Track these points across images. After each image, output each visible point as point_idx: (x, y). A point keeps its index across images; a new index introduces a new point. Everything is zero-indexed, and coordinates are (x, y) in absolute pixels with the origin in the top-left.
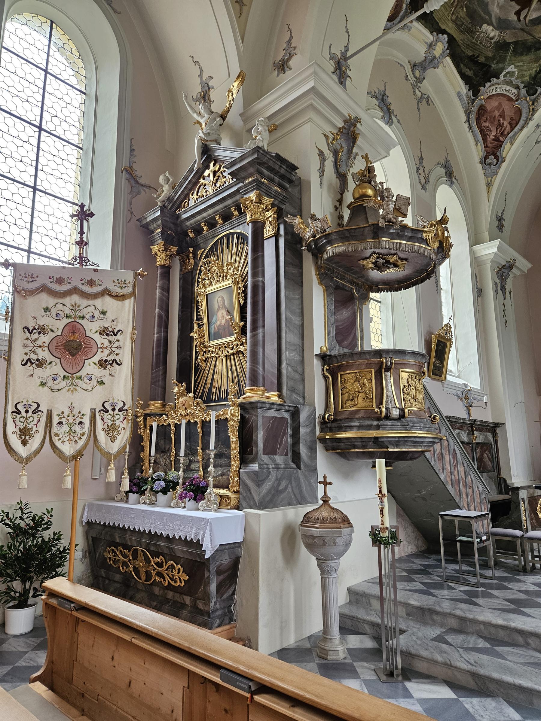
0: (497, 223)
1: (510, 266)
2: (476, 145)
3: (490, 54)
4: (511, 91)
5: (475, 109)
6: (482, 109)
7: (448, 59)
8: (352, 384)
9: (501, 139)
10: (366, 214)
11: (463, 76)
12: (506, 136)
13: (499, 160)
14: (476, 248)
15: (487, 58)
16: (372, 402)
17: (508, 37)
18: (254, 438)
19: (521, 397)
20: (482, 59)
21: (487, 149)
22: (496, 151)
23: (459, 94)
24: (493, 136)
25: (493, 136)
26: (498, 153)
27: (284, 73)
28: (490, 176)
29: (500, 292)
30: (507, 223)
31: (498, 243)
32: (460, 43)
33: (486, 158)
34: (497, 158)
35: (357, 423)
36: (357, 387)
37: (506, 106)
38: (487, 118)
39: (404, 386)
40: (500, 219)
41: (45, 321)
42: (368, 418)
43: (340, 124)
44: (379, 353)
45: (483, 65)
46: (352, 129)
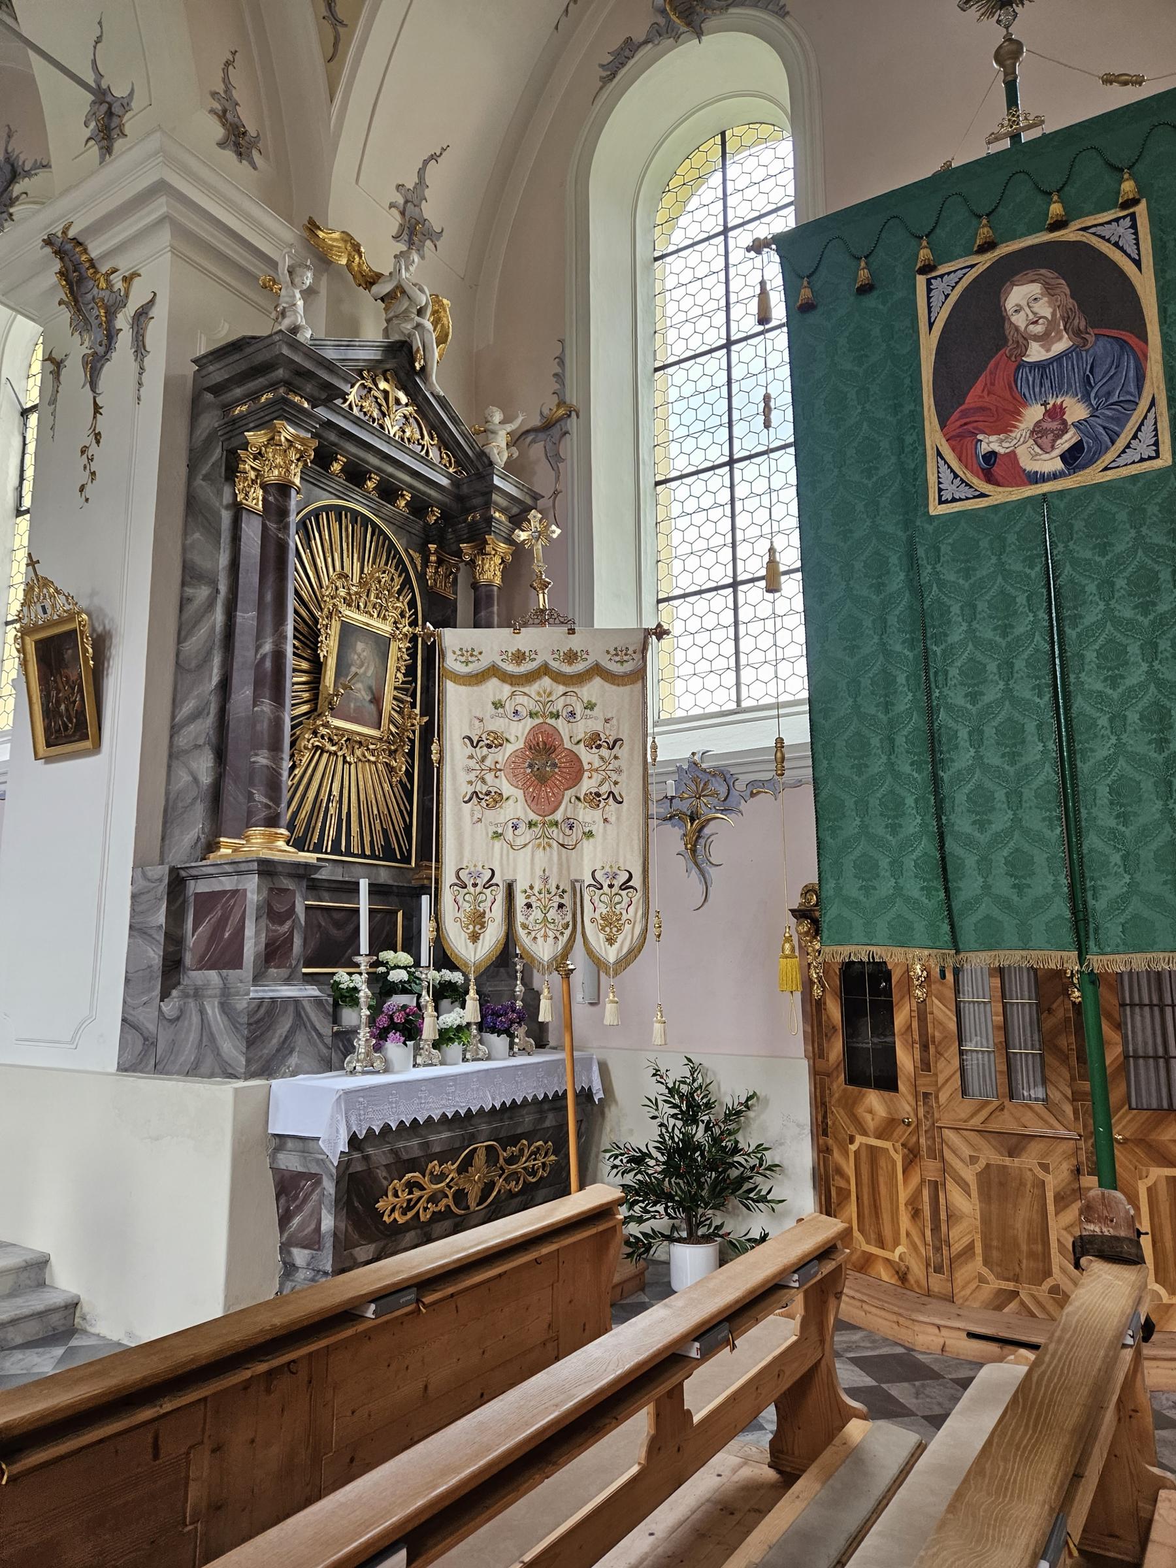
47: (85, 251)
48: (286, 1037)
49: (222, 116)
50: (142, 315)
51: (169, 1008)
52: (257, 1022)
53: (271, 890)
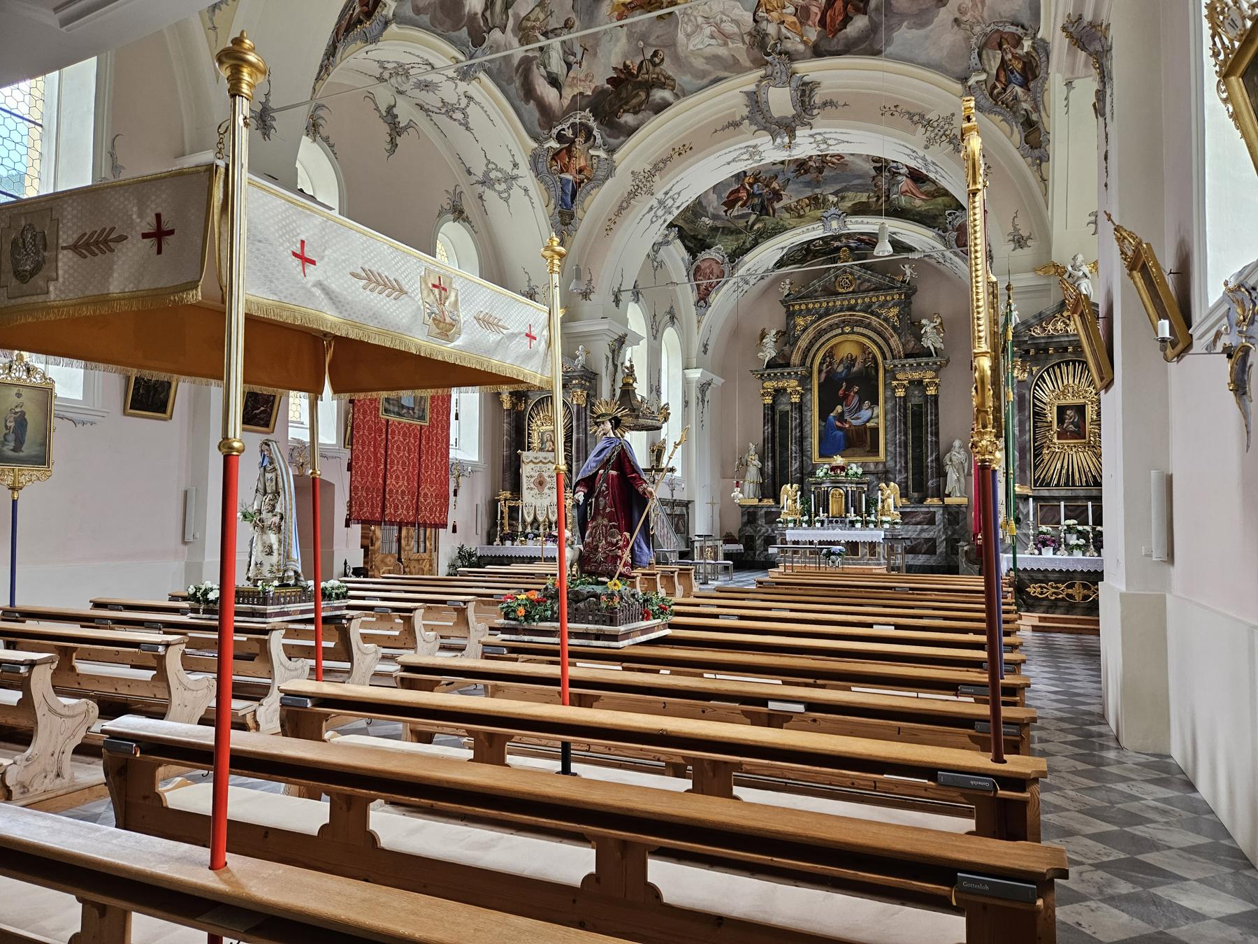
3: (706, 234)
4: (719, 258)
5: (694, 267)
6: (698, 268)
7: (678, 241)
11: (687, 248)
13: (707, 305)
15: (704, 236)
17: (719, 224)
19: (708, 482)
20: (700, 237)
23: (683, 259)
28: (701, 315)
29: (700, 403)
32: (686, 229)
33: (698, 302)
34: (706, 303)
37: (715, 266)
40: (705, 346)
41: (533, 473)
43: (616, 337)
45: (701, 240)
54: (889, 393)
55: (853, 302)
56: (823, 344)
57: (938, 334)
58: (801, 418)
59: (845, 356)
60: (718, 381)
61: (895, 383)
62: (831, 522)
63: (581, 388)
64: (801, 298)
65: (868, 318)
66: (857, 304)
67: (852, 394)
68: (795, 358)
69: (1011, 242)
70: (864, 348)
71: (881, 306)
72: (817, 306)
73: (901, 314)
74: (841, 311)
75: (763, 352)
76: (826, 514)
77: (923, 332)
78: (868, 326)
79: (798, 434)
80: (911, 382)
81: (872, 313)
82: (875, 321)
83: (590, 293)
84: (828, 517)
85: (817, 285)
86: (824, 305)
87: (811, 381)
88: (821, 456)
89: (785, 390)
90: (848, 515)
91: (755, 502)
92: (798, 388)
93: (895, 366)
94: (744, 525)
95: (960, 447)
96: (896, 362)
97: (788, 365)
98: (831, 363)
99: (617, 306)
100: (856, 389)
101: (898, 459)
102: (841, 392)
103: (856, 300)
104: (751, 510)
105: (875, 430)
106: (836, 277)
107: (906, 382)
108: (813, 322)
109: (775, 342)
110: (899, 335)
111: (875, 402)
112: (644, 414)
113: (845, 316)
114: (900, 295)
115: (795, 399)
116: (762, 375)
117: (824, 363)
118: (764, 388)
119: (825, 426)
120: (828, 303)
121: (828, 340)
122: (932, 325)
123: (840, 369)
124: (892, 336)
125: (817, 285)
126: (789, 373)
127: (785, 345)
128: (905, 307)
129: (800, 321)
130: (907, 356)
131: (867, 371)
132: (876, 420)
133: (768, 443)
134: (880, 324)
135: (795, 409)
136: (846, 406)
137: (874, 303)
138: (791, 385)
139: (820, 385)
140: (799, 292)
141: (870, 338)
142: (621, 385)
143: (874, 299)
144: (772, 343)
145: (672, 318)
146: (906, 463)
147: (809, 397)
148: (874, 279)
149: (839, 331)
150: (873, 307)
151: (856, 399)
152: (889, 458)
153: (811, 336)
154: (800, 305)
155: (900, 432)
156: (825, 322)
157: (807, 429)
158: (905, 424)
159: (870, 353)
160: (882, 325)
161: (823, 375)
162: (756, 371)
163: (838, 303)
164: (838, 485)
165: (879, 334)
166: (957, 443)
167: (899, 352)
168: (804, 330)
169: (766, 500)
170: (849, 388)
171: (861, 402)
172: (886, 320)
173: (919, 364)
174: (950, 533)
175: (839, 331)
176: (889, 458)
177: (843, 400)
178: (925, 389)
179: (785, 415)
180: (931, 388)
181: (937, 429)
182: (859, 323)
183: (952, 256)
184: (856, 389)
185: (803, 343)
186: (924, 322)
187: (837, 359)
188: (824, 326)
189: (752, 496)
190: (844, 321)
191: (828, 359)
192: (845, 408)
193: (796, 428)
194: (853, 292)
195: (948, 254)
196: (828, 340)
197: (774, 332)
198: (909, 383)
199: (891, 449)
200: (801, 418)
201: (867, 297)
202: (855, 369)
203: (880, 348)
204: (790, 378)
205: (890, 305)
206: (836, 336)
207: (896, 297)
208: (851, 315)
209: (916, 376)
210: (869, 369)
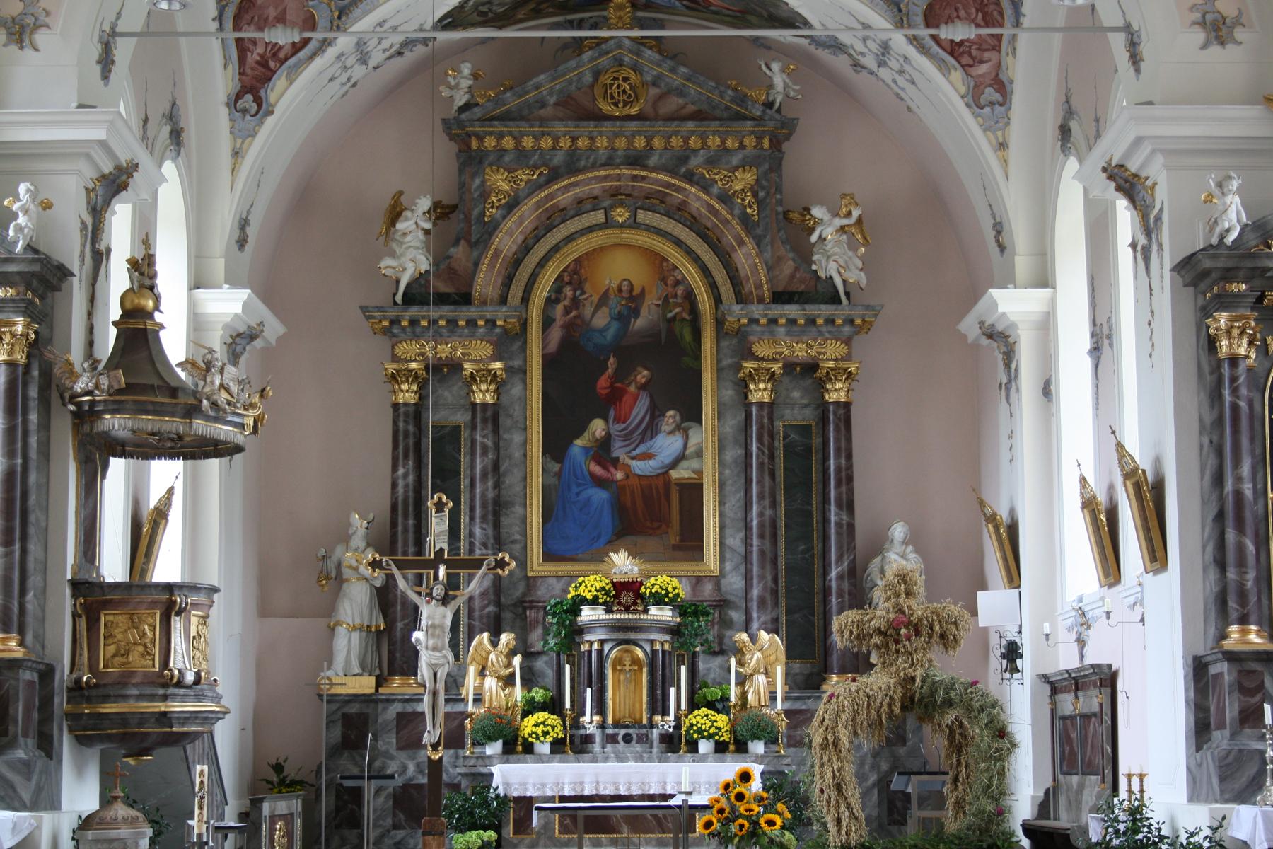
0: (237, 233)
1: (252, 336)
2: (225, 66)
8: (126, 631)
9: (272, 64)
10: (149, 348)
12: (283, 62)
13: (262, 109)
14: (201, 293)
16: (153, 660)
18: (11, 712)
21: (244, 77)
22: (258, 85)
24: (258, 54)
25: (258, 54)
26: (262, 93)
27: (22, 48)
28: (240, 137)
30: (251, 231)
31: (245, 297)
33: (238, 97)
34: (258, 101)
35: (135, 692)
36: (134, 637)
38: (253, 18)
39: (194, 638)
42: (152, 684)
43: (107, 168)
44: (169, 588)
46: (124, 177)
47: (1127, 170)
48: (1254, 778)
49: (1202, 24)
50: (1158, 219)
51: (1198, 756)
52: (1227, 765)
53: (1240, 672)
54: (729, 393)
55: (640, 143)
56: (556, 249)
57: (852, 246)
58: (497, 447)
59: (615, 284)
60: (274, 328)
61: (750, 365)
62: (612, 739)
63: (25, 313)
64: (505, 118)
65: (679, 189)
66: (650, 147)
67: (632, 388)
68: (485, 282)
69: (1197, 28)
70: (659, 263)
71: (712, 162)
72: (546, 143)
73: (763, 188)
74: (609, 163)
75: (393, 254)
76: (596, 718)
77: (814, 238)
78: (679, 212)
79: (491, 494)
80: (789, 367)
81: (690, 177)
82: (696, 199)
83: (37, 27)
84: (602, 726)
85: (544, 91)
86: (565, 143)
87: (523, 348)
88: (548, 556)
89: (456, 367)
90: (658, 718)
91: (365, 684)
92: (498, 365)
93: (756, 321)
94: (334, 752)
95: (905, 543)
96: (756, 310)
97: (465, 299)
98: (575, 303)
99: (105, 76)
100: (643, 375)
101: (755, 569)
102: (603, 383)
103: (649, 140)
104: (354, 709)
105: (693, 491)
106: (597, 74)
107: (776, 367)
108: (537, 187)
109: (427, 232)
110: (759, 241)
111: (692, 414)
112: (214, 405)
113: (619, 178)
114: (759, 138)
115: (483, 394)
116: (395, 322)
117: (557, 301)
118: (395, 358)
119: (559, 475)
120: (574, 139)
121: (569, 239)
122: (838, 222)
123: (601, 320)
124: (741, 243)
125: (544, 91)
126: (472, 323)
127: (456, 243)
128: (771, 170)
129: (500, 181)
130: (781, 297)
131: (670, 331)
132: (694, 464)
133: (406, 517)
134: (711, 209)
135: (485, 421)
136: (618, 420)
137: (695, 151)
138: (475, 354)
139: (549, 363)
140: (498, 101)
141: (678, 243)
142: (115, 313)
143: (694, 142)
144: (420, 235)
145: (177, 135)
146: (775, 580)
147: (516, 390)
148: (693, 89)
149: (599, 217)
150: (694, 162)
151: (640, 409)
152: (728, 566)
153: (528, 224)
154: (500, 136)
155: (761, 497)
156: (566, 189)
157: (513, 480)
158: (773, 475)
159: (677, 283)
160: (715, 212)
161: (556, 334)
162: (379, 309)
163: (602, 142)
164: (632, 636)
165: (703, 234)
166: (898, 531)
167: (759, 286)
168: (512, 205)
169: (397, 681)
170: (624, 373)
171: (655, 413)
172: (725, 198)
173: (811, 321)
174: (885, 767)
175: (599, 217)
176: (728, 566)
177: (609, 404)
178: (821, 386)
179: (448, 438)
180: (839, 385)
181: (851, 491)
182: (656, 201)
183: (911, 51)
184: (643, 375)
185: (506, 240)
186: (817, 212)
187: (592, 294)
188: (565, 199)
189: (357, 670)
190: (615, 193)
191: (568, 291)
192: (616, 428)
193: (484, 476)
194: (639, 117)
195: (899, 40)
196: (569, 239)
197: (425, 204)
198: (785, 367)
199: (735, 541)
200: (497, 447)
201: (676, 133)
202: (639, 323)
203: (705, 271)
204: (472, 336)
205: (735, 161)
206: (591, 229)
207: (602, 142)
208: (635, 178)
209: (801, 352)
210: (677, 327)
